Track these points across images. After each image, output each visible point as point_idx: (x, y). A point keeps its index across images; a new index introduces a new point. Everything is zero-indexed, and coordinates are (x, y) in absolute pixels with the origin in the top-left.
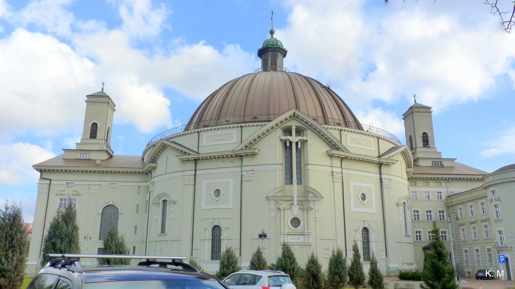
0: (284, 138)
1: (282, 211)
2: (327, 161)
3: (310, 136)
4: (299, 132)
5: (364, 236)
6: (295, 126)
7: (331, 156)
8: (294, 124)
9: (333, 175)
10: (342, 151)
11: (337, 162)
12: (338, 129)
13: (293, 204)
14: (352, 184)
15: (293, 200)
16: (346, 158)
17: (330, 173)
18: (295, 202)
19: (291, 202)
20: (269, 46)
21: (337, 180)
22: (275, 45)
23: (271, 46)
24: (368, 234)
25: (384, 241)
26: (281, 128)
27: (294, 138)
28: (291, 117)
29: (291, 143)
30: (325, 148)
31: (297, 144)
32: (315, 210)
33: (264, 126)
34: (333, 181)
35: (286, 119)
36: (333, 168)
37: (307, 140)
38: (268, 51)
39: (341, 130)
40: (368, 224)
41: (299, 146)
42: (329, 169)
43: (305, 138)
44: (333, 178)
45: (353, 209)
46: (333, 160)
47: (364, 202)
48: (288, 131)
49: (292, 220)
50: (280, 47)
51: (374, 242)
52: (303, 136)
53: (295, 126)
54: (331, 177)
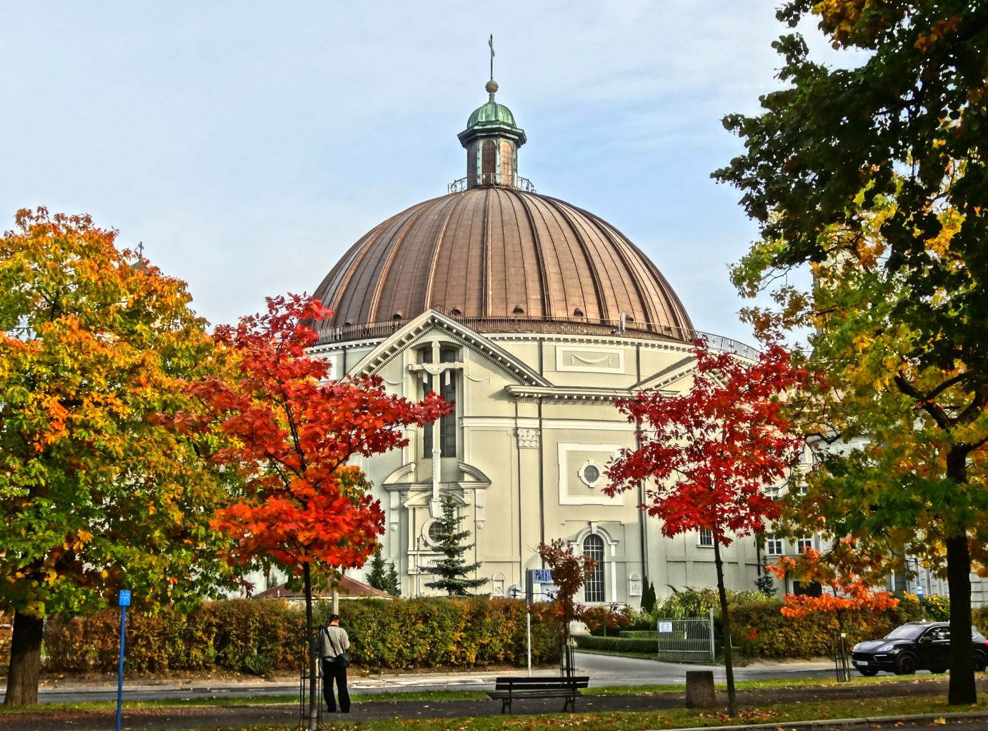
0: (417, 367)
1: (411, 512)
2: (506, 407)
3: (468, 362)
4: (449, 352)
5: (593, 553)
6: (440, 342)
7: (513, 397)
8: (436, 338)
9: (517, 435)
10: (538, 385)
11: (529, 408)
12: (534, 339)
13: (432, 496)
14: (564, 448)
15: (432, 489)
16: (549, 397)
17: (511, 432)
18: (436, 493)
19: (428, 494)
20: (476, 128)
21: (527, 444)
22: (492, 123)
23: (481, 128)
24: (602, 548)
25: (640, 560)
26: (412, 348)
27: (436, 367)
28: (427, 325)
29: (430, 376)
30: (501, 382)
31: (442, 376)
32: (475, 506)
33: (377, 346)
34: (518, 448)
35: (418, 331)
36: (518, 421)
37: (461, 370)
38: (476, 139)
39: (542, 339)
40: (598, 527)
41: (448, 382)
42: (511, 423)
43: (457, 365)
44: (518, 442)
45: (565, 499)
46: (518, 404)
47: (592, 485)
48: (424, 352)
49: (431, 527)
50: (502, 126)
51: (613, 564)
52: (453, 361)
53: (440, 342)
54: (514, 440)
